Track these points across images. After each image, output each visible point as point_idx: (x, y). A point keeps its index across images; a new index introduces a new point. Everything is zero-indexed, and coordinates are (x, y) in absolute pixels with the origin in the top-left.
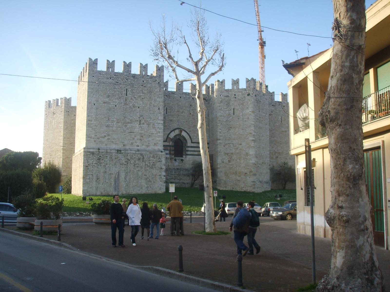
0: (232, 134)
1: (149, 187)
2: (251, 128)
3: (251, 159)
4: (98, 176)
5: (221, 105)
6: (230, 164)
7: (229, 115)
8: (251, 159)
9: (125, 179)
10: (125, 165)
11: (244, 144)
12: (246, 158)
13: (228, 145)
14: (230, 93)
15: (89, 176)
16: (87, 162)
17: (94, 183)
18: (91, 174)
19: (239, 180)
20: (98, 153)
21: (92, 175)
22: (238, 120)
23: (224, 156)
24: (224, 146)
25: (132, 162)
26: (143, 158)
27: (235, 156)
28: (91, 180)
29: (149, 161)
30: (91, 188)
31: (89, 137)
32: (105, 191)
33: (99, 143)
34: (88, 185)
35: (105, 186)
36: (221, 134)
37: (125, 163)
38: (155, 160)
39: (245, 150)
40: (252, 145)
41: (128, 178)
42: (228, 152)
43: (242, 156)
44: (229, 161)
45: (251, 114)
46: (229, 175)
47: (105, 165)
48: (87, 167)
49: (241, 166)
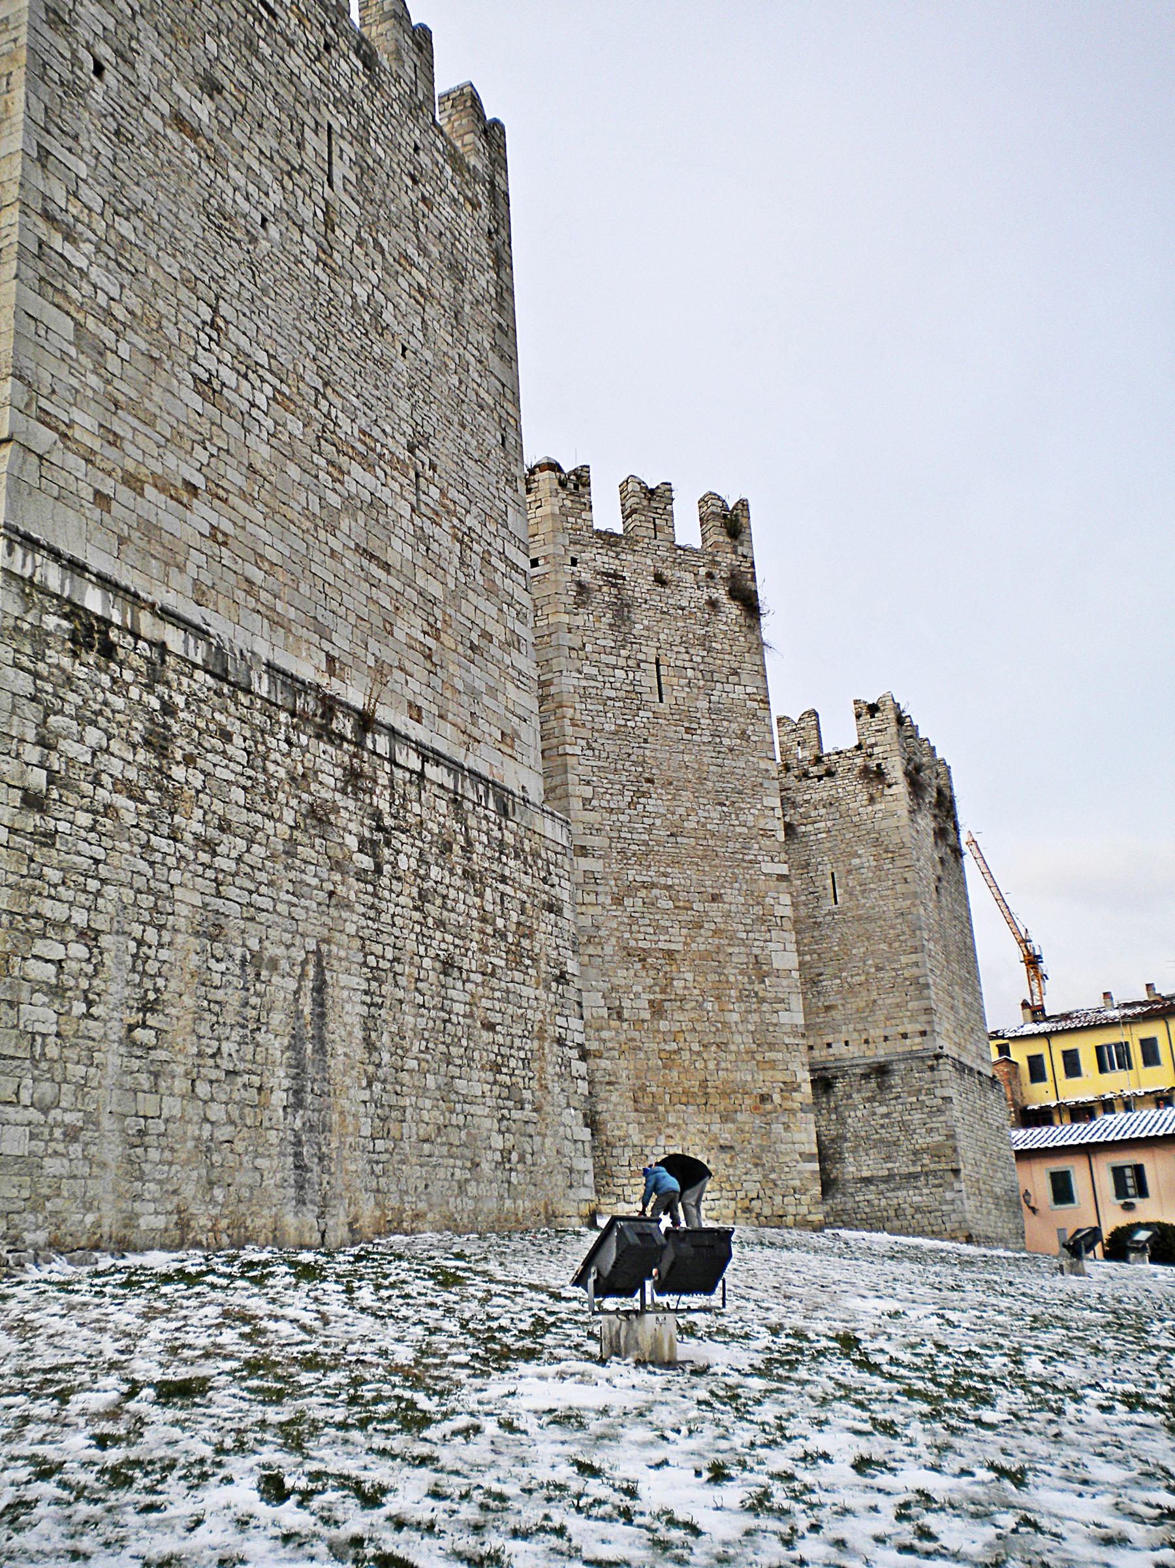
0: (658, 822)
1: (514, 1157)
2: (767, 802)
3: (782, 1001)
4: (152, 967)
5: (579, 621)
6: (663, 1025)
7: (633, 699)
8: (782, 1001)
9: (370, 1046)
10: (361, 875)
11: (733, 897)
12: (756, 993)
13: (643, 893)
14: (630, 557)
15: (58, 952)
16: (42, 742)
17: (112, 1057)
18: (80, 918)
19: (732, 1148)
20: (148, 660)
21: (89, 935)
22: (686, 736)
23: (622, 973)
24: (618, 901)
25: (403, 862)
26: (468, 841)
27: (689, 976)
28: (80, 1008)
29: (501, 886)
30: (72, 1135)
31: (45, 418)
32: (218, 1193)
33: (135, 535)
34: (47, 1090)
35: (216, 1112)
36: (591, 817)
37: (366, 862)
38: (527, 880)
39: (744, 935)
40: (779, 911)
41: (386, 1038)
42: (641, 944)
43: (732, 978)
44: (657, 1010)
45: (759, 713)
46: (661, 1108)
47: (213, 833)
48: (33, 801)
49: (733, 1048)
